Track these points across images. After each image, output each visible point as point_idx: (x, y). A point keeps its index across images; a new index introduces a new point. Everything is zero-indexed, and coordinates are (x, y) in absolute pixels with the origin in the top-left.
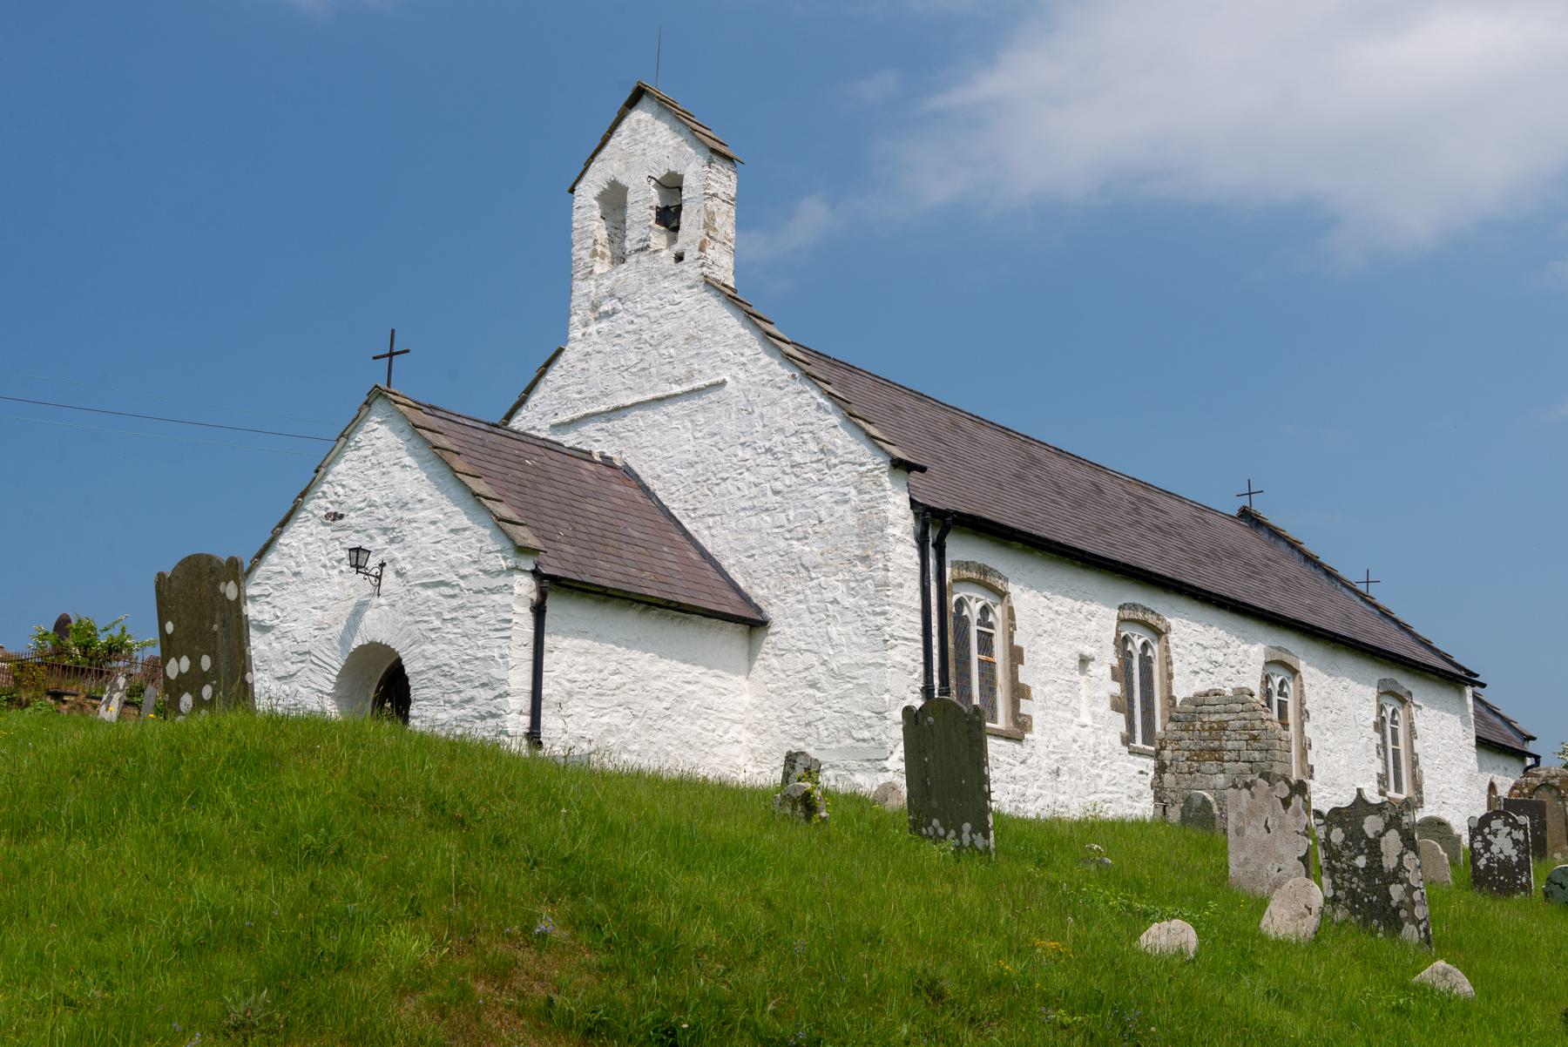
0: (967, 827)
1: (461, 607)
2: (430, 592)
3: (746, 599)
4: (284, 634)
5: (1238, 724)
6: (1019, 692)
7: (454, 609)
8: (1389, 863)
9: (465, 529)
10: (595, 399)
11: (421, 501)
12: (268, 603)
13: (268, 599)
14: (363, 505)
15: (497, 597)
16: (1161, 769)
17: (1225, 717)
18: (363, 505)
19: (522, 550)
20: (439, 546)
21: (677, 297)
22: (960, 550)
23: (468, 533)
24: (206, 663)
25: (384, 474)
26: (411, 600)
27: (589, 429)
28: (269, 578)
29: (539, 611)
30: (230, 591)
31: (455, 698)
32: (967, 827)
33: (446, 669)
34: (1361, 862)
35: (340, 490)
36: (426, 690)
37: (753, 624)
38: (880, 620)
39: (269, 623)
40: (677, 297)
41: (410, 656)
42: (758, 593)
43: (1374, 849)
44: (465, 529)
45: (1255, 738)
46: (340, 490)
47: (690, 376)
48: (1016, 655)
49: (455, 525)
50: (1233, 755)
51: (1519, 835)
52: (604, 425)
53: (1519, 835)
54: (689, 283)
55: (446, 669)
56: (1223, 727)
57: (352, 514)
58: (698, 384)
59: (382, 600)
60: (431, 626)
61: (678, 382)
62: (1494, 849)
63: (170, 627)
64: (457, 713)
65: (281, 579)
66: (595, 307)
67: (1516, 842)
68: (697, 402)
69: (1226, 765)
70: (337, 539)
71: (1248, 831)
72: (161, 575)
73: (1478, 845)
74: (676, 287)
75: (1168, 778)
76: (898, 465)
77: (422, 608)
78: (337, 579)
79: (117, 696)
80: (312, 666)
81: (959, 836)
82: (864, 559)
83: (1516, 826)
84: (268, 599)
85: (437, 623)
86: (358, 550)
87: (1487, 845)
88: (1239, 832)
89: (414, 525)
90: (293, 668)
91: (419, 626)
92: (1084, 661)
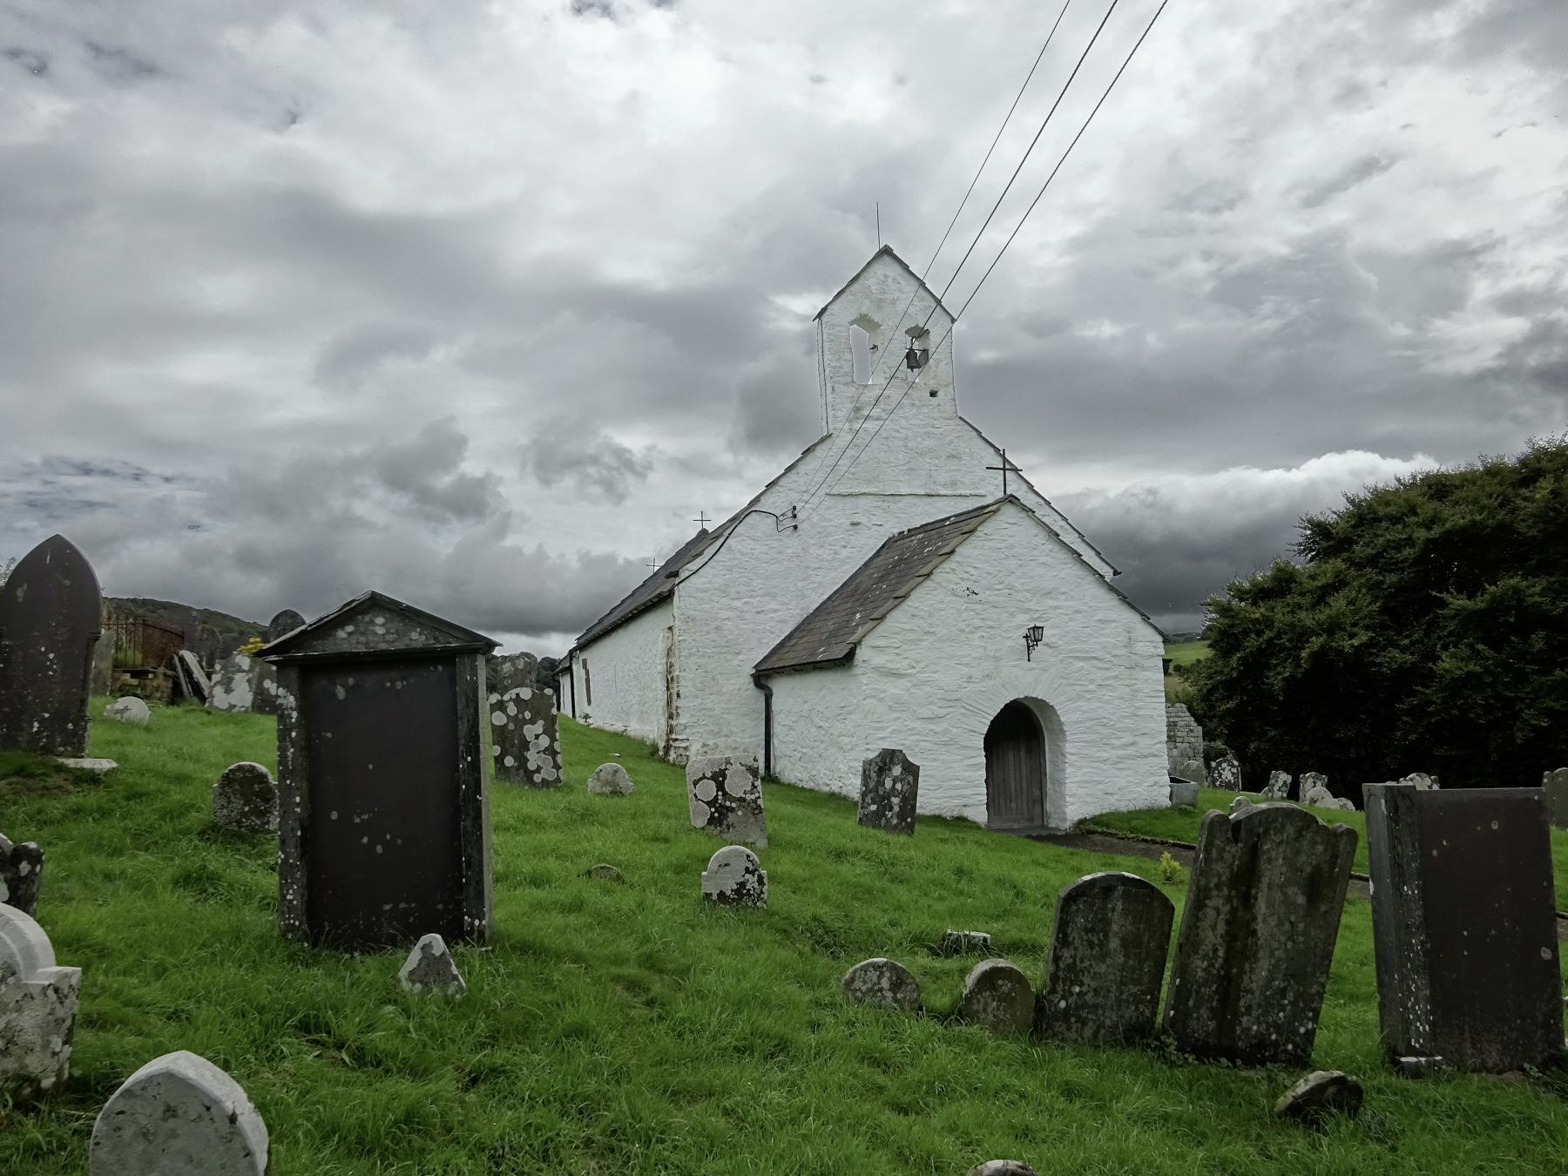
1: (1115, 677)
2: (1080, 664)
4: (925, 683)
5: (1183, 723)
7: (1108, 679)
9: (1112, 621)
10: (869, 482)
11: (1064, 593)
12: (898, 654)
13: (897, 651)
14: (1000, 586)
15: (1148, 674)
17: (1176, 719)
18: (1000, 586)
20: (1087, 630)
21: (937, 423)
23: (1114, 624)
25: (1021, 565)
26: (1066, 669)
28: (896, 633)
31: (1117, 742)
33: (1105, 721)
35: (970, 569)
36: (1084, 735)
39: (902, 672)
40: (937, 423)
41: (1066, 709)
44: (1112, 621)
45: (1191, 731)
46: (970, 569)
47: (954, 484)
49: (1100, 616)
50: (1181, 740)
51: (1235, 770)
52: (879, 504)
53: (1235, 770)
54: (944, 415)
55: (1105, 721)
57: (987, 592)
58: (968, 492)
59: (1032, 664)
60: (1086, 689)
61: (945, 486)
62: (1223, 777)
64: (1121, 752)
65: (913, 636)
66: (857, 409)
67: (1233, 774)
69: (1178, 745)
70: (973, 610)
73: (1216, 775)
74: (935, 415)
77: (1077, 675)
78: (978, 643)
80: (963, 711)
83: (1233, 766)
84: (897, 651)
85: (1091, 687)
86: (1035, 628)
87: (1220, 775)
89: (1060, 611)
90: (942, 712)
91: (1077, 688)
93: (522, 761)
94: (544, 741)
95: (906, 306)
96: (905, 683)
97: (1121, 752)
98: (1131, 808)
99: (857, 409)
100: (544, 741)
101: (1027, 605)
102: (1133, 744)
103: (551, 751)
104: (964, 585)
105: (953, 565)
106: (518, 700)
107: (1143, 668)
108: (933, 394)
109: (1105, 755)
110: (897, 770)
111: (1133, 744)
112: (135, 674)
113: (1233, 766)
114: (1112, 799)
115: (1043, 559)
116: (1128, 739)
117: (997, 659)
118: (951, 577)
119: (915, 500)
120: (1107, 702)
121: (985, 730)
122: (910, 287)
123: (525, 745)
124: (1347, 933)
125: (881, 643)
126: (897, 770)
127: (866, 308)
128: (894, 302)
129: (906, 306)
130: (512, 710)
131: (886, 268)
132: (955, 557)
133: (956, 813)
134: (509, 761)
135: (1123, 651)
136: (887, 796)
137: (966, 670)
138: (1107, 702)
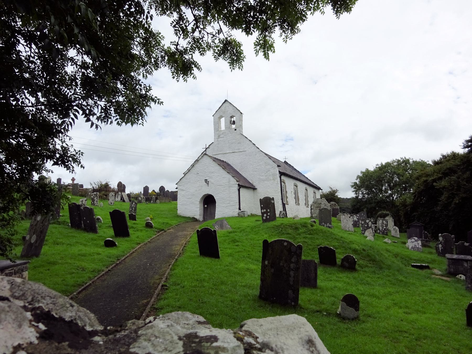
0: (328, 224)
1: (226, 189)
2: (219, 187)
3: (253, 185)
6: (287, 197)
8: (370, 226)
16: (311, 209)
19: (237, 181)
22: (283, 177)
24: (269, 210)
27: (219, 156)
29: (239, 190)
30: (273, 202)
32: (328, 224)
34: (366, 226)
37: (254, 189)
38: (277, 189)
42: (254, 184)
43: (368, 224)
47: (239, 149)
48: (286, 192)
51: (358, 217)
53: (358, 217)
56: (321, 203)
61: (237, 150)
63: (262, 206)
64: (227, 205)
66: (219, 136)
68: (241, 153)
71: (344, 221)
72: (260, 199)
75: (312, 210)
76: (278, 166)
79: (119, 196)
81: (327, 225)
82: (273, 179)
83: (357, 216)
85: (221, 191)
86: (206, 180)
88: (343, 221)
90: (191, 197)
92: (292, 192)
93: (94, 202)
94: (96, 200)
95: (231, 111)
96: (185, 192)
97: (227, 205)
98: (228, 216)
99: (219, 136)
100: (96, 200)
101: (209, 175)
102: (229, 203)
103: (97, 201)
104: (196, 172)
105: (194, 168)
106: (94, 194)
107: (232, 187)
108: (235, 130)
109: (224, 206)
110: (134, 203)
111: (229, 203)
112: (106, 196)
113: (357, 216)
114: (224, 215)
115: (212, 166)
116: (228, 202)
117: (202, 186)
118: (194, 171)
119: (230, 154)
120: (224, 194)
121: (199, 200)
122: (231, 107)
123: (94, 200)
124: (259, 245)
125: (181, 184)
126: (134, 203)
127: (221, 114)
128: (227, 111)
129: (231, 111)
130: (94, 195)
131: (226, 104)
132: (195, 167)
133: (193, 217)
134: (93, 203)
135: (228, 184)
136: (132, 208)
137: (196, 189)
138: (224, 194)
